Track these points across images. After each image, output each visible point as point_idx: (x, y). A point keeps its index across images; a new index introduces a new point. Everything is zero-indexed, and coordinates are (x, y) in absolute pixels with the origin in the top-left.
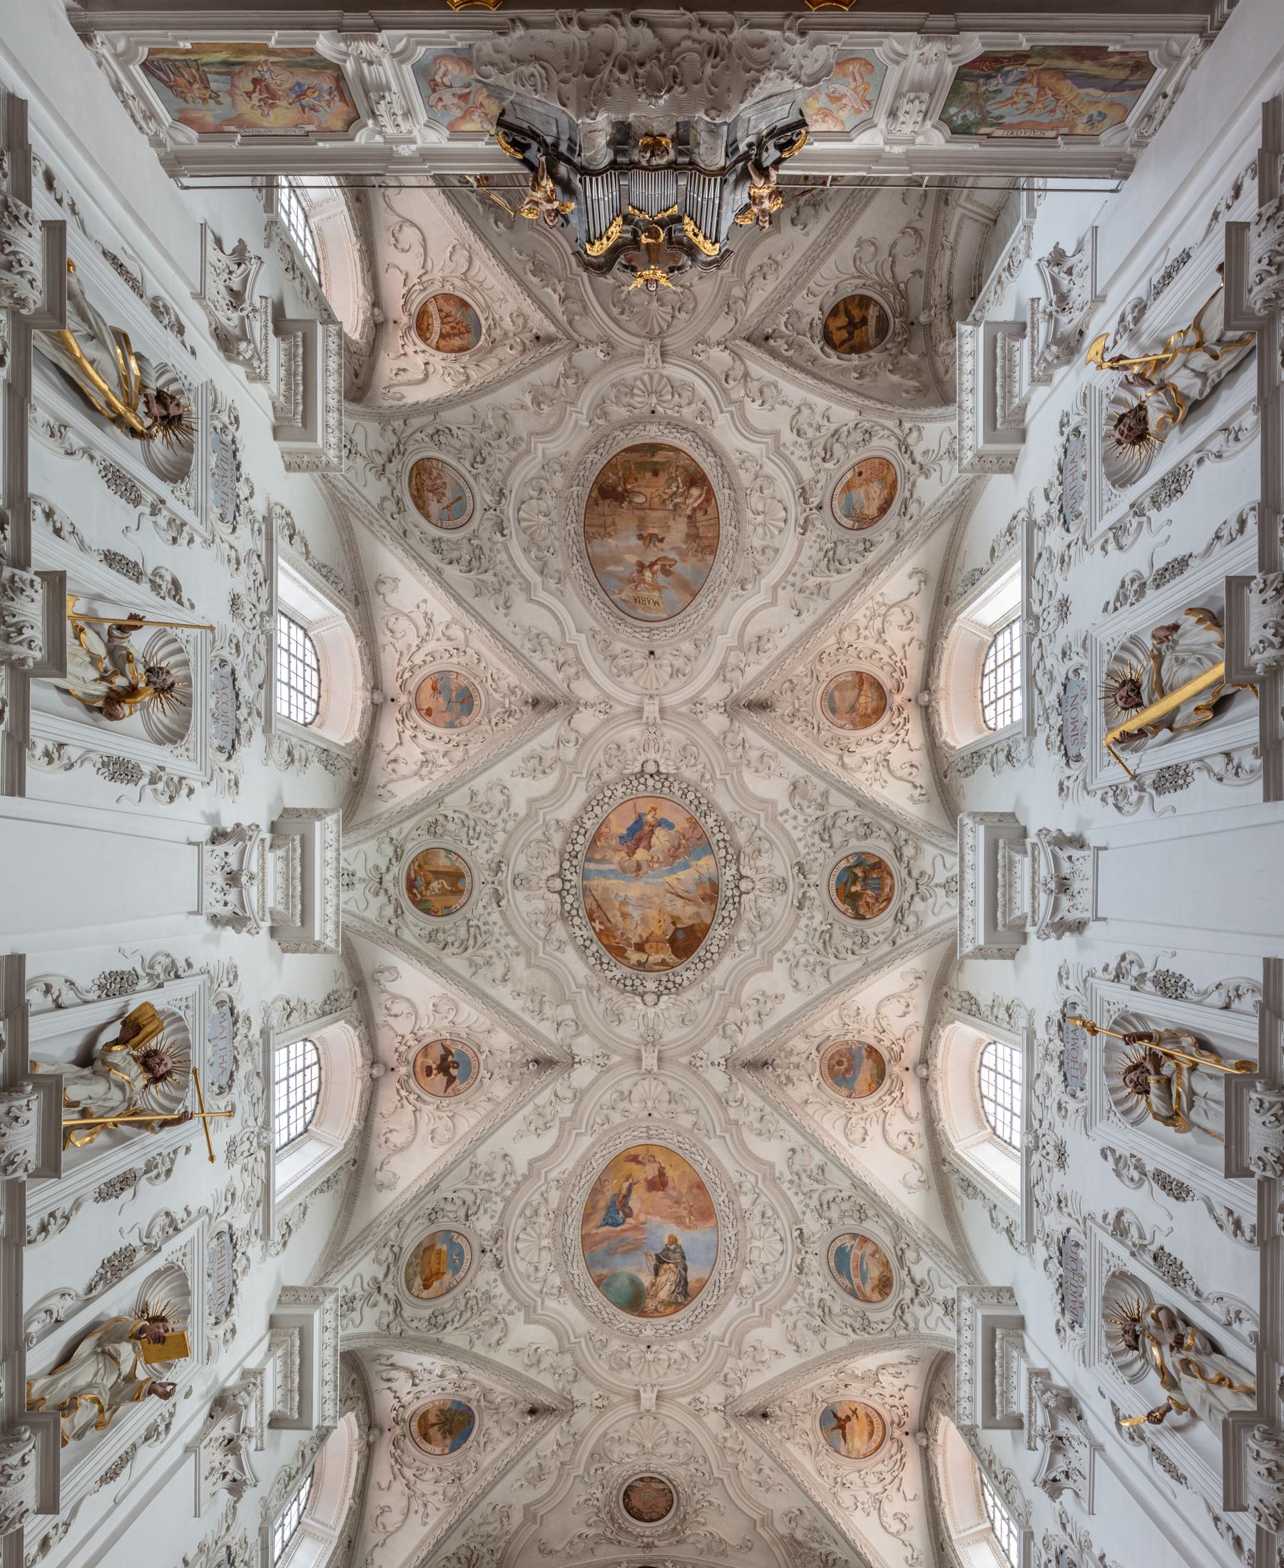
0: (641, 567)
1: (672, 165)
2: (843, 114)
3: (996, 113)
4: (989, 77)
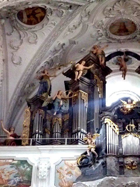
1: (125, 157)
2: (66, 167)
3: (14, 169)
4: (20, 182)
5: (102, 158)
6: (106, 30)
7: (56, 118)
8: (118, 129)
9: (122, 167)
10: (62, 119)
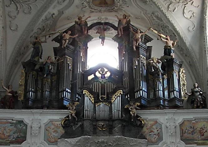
1: (98, 121)
2: (53, 127)
3: (13, 127)
4: (18, 137)
5: (80, 121)
6: (89, 3)
7: (46, 79)
8: (93, 99)
10: (51, 80)
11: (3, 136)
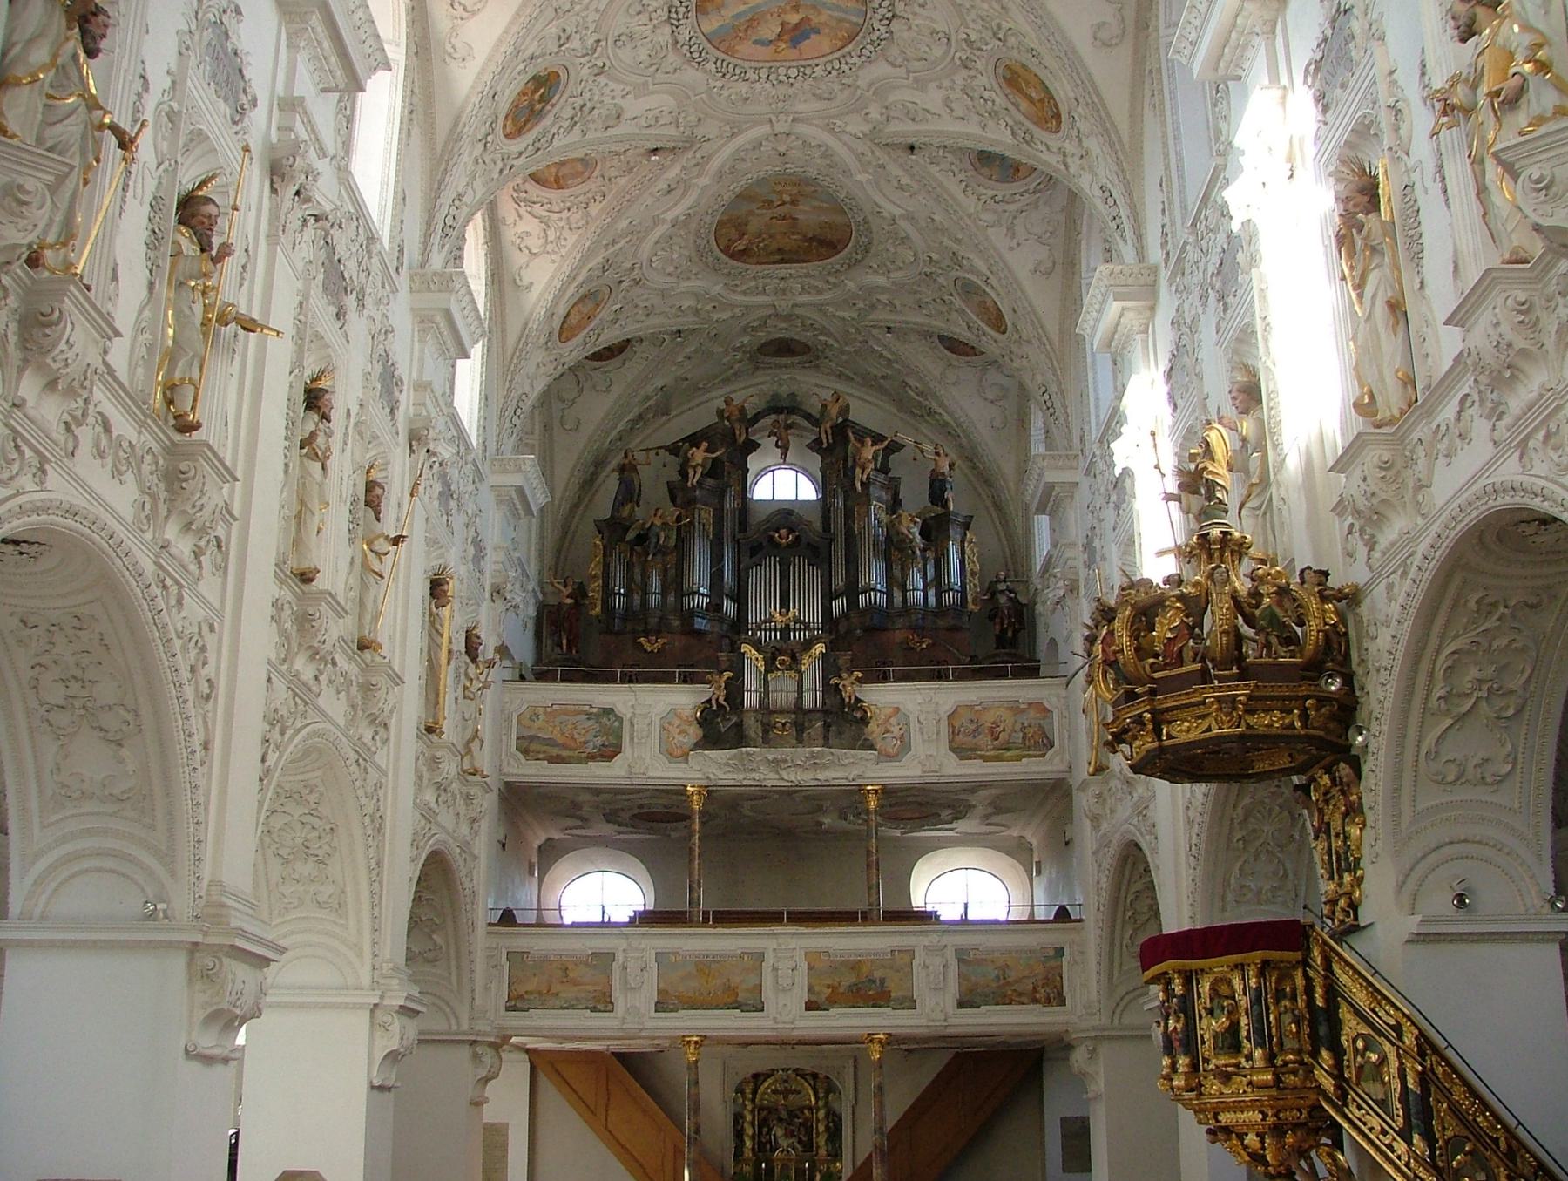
0: (794, 202)
2: (678, 722)
3: (592, 722)
9: (767, 728)
11: (571, 743)
